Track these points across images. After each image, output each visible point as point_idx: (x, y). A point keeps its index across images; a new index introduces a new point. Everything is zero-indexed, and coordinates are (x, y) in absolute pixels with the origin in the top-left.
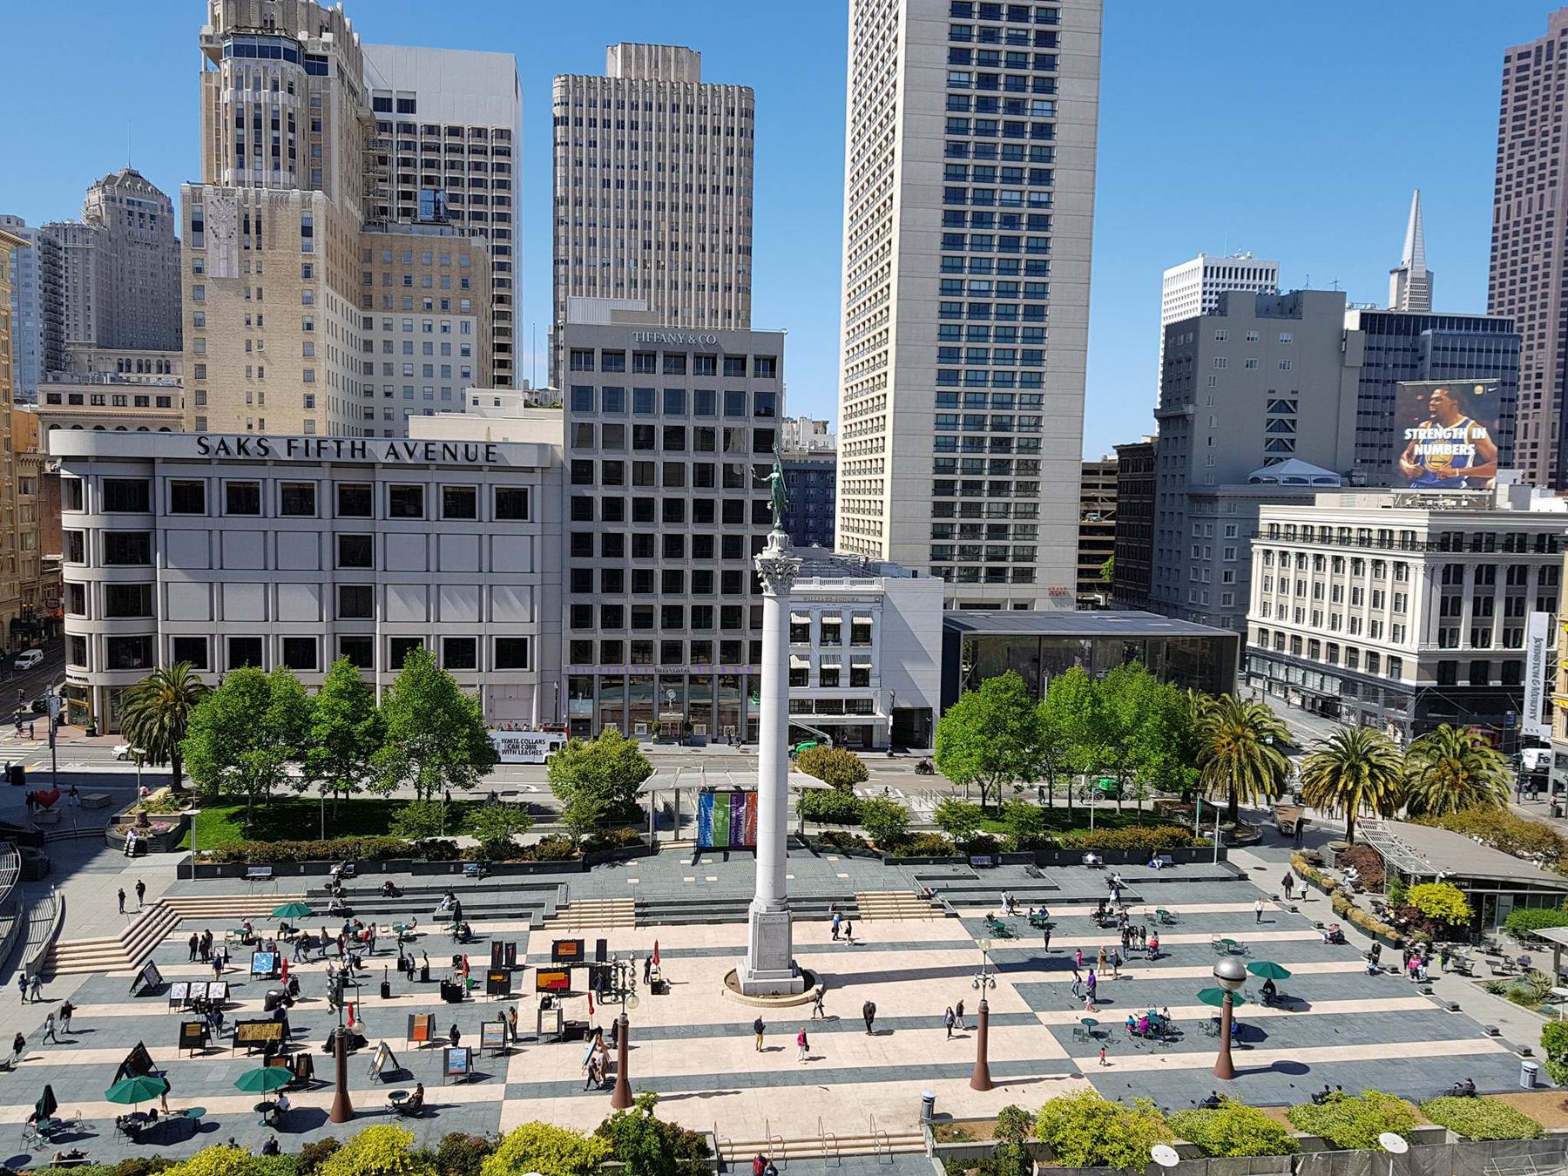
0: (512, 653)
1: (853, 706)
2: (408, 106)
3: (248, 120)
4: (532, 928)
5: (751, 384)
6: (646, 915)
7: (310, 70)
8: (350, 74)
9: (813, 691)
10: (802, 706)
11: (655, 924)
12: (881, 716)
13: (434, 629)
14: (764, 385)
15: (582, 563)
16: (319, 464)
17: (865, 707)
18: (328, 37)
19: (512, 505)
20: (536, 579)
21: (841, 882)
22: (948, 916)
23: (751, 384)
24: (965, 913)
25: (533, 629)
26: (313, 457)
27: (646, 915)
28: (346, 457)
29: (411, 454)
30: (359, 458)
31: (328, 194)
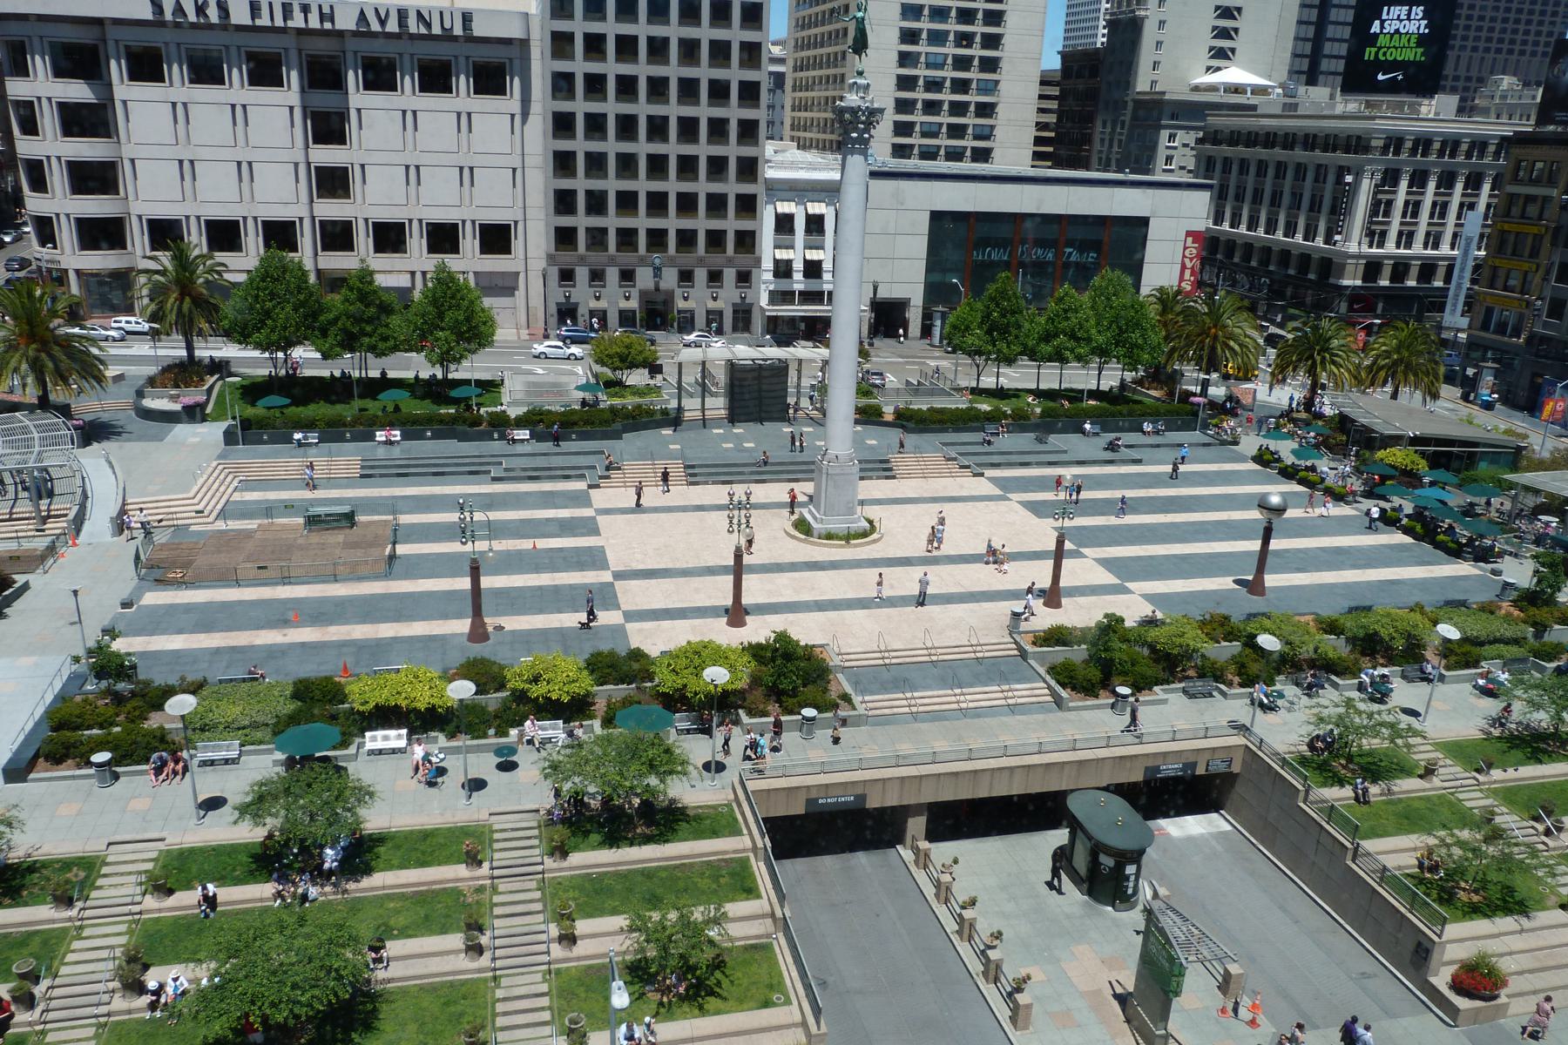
0: (496, 238)
4: (590, 487)
6: (694, 475)
11: (706, 483)
13: (416, 214)
15: (565, 145)
16: (284, 30)
19: (490, 80)
20: (518, 164)
21: (871, 447)
22: (975, 475)
24: (989, 473)
25: (520, 217)
26: (279, 22)
27: (694, 475)
28: (314, 23)
29: (383, 22)
30: (327, 26)
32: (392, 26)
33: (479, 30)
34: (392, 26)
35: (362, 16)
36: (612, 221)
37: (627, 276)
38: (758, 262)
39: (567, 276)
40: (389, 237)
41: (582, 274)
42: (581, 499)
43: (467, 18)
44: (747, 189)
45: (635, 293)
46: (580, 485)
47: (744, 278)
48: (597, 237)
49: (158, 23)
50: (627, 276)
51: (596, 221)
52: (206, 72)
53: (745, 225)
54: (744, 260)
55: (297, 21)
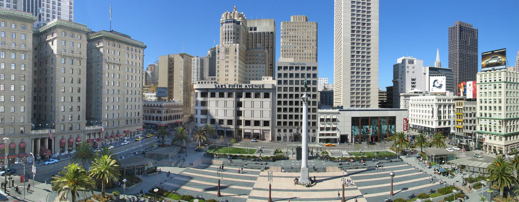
0: (266, 123)
1: (333, 135)
2: (255, 29)
3: (227, 33)
5: (311, 72)
7: (237, 24)
8: (244, 24)
9: (325, 132)
10: (323, 135)
12: (338, 136)
13: (252, 119)
14: (314, 72)
17: (335, 135)
18: (240, 18)
20: (270, 109)
23: (311, 72)
31: (240, 44)
32: (251, 87)
33: (265, 87)
34: (251, 87)
35: (246, 86)
36: (288, 120)
37: (291, 131)
38: (317, 128)
39: (279, 131)
40: (248, 123)
41: (282, 130)
42: (258, 173)
43: (263, 85)
44: (314, 114)
45: (292, 134)
46: (260, 170)
47: (314, 131)
48: (285, 123)
49: (216, 89)
50: (291, 131)
51: (285, 120)
52: (222, 95)
53: (314, 121)
54: (314, 128)
55: (236, 87)
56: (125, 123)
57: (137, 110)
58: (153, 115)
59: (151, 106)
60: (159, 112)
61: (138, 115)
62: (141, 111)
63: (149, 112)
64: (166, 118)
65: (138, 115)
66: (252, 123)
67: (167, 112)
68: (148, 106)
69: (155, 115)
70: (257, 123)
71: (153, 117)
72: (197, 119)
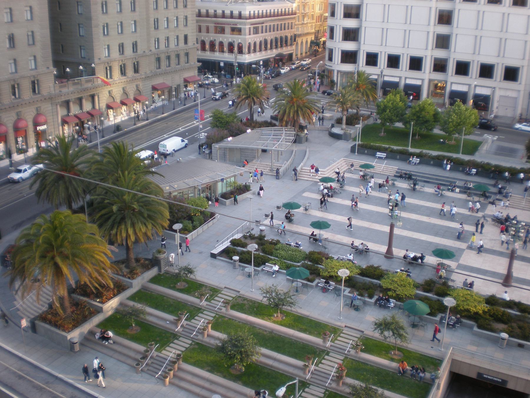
40: (462, 68)
56: (153, 66)
57: (182, 31)
58: (219, 38)
59: (215, 16)
60: (236, 30)
61: (186, 42)
62: (191, 31)
63: (212, 29)
64: (253, 49)
65: (186, 42)
66: (474, 70)
67: (256, 31)
68: (207, 15)
69: (227, 38)
70: (486, 71)
71: (221, 44)
72: (331, 51)
